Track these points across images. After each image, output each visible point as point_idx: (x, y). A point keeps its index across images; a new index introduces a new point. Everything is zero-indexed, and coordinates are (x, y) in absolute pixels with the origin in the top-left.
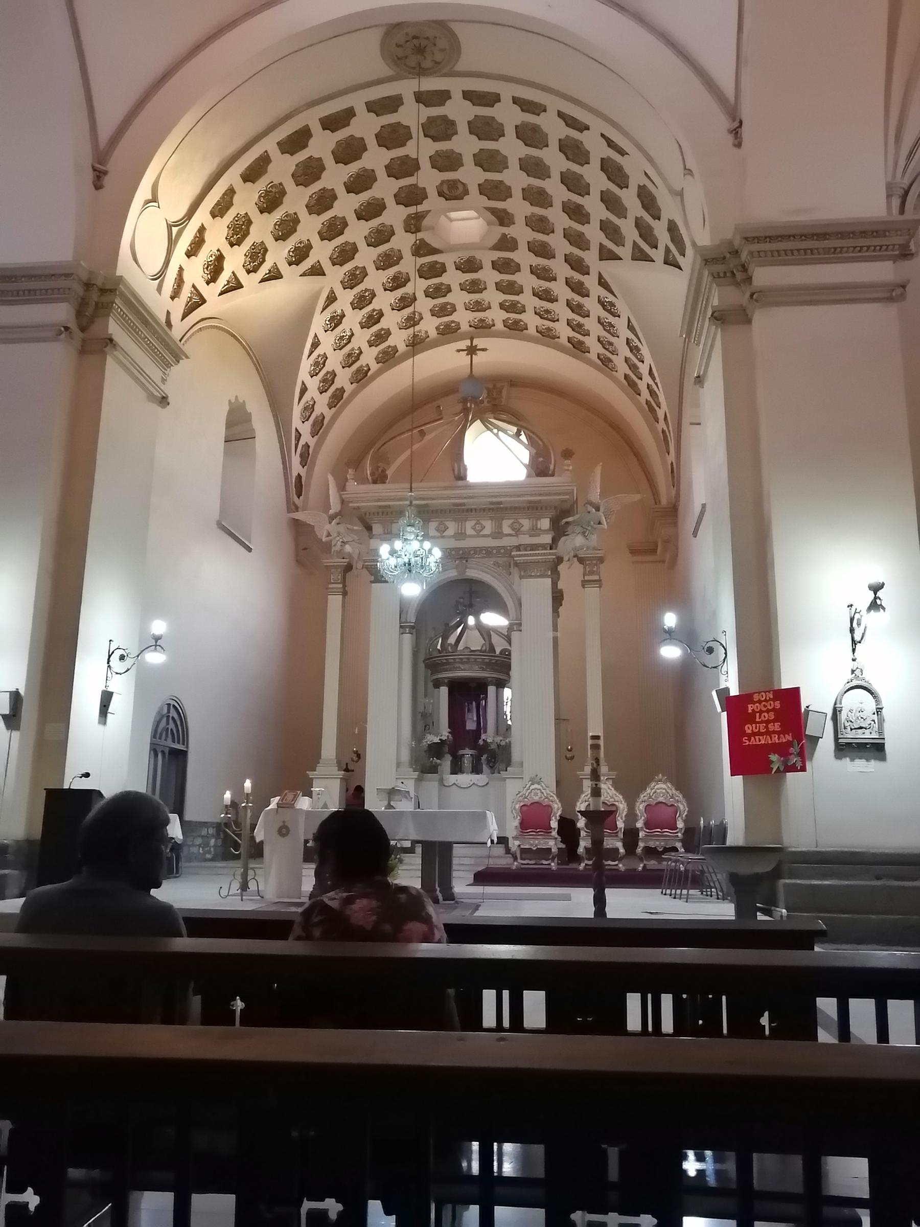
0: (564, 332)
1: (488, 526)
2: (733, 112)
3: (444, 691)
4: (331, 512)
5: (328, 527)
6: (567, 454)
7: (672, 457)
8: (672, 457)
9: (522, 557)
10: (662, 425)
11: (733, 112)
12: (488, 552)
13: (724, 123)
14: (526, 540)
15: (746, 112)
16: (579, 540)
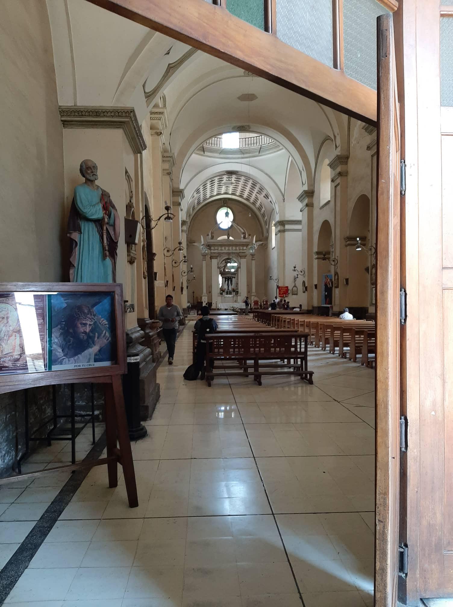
0: (245, 196)
1: (234, 248)
2: (283, 196)
3: (224, 279)
4: (202, 243)
5: (201, 247)
6: (249, 235)
7: (267, 227)
8: (267, 227)
9: (241, 254)
10: (265, 219)
11: (283, 196)
12: (234, 253)
13: (282, 197)
14: (241, 251)
15: (285, 197)
16: (251, 251)
